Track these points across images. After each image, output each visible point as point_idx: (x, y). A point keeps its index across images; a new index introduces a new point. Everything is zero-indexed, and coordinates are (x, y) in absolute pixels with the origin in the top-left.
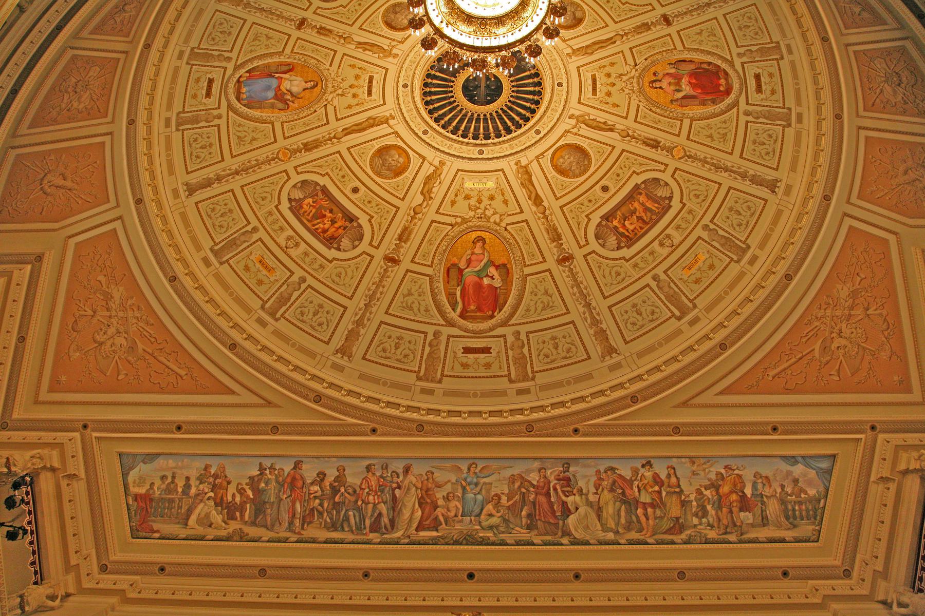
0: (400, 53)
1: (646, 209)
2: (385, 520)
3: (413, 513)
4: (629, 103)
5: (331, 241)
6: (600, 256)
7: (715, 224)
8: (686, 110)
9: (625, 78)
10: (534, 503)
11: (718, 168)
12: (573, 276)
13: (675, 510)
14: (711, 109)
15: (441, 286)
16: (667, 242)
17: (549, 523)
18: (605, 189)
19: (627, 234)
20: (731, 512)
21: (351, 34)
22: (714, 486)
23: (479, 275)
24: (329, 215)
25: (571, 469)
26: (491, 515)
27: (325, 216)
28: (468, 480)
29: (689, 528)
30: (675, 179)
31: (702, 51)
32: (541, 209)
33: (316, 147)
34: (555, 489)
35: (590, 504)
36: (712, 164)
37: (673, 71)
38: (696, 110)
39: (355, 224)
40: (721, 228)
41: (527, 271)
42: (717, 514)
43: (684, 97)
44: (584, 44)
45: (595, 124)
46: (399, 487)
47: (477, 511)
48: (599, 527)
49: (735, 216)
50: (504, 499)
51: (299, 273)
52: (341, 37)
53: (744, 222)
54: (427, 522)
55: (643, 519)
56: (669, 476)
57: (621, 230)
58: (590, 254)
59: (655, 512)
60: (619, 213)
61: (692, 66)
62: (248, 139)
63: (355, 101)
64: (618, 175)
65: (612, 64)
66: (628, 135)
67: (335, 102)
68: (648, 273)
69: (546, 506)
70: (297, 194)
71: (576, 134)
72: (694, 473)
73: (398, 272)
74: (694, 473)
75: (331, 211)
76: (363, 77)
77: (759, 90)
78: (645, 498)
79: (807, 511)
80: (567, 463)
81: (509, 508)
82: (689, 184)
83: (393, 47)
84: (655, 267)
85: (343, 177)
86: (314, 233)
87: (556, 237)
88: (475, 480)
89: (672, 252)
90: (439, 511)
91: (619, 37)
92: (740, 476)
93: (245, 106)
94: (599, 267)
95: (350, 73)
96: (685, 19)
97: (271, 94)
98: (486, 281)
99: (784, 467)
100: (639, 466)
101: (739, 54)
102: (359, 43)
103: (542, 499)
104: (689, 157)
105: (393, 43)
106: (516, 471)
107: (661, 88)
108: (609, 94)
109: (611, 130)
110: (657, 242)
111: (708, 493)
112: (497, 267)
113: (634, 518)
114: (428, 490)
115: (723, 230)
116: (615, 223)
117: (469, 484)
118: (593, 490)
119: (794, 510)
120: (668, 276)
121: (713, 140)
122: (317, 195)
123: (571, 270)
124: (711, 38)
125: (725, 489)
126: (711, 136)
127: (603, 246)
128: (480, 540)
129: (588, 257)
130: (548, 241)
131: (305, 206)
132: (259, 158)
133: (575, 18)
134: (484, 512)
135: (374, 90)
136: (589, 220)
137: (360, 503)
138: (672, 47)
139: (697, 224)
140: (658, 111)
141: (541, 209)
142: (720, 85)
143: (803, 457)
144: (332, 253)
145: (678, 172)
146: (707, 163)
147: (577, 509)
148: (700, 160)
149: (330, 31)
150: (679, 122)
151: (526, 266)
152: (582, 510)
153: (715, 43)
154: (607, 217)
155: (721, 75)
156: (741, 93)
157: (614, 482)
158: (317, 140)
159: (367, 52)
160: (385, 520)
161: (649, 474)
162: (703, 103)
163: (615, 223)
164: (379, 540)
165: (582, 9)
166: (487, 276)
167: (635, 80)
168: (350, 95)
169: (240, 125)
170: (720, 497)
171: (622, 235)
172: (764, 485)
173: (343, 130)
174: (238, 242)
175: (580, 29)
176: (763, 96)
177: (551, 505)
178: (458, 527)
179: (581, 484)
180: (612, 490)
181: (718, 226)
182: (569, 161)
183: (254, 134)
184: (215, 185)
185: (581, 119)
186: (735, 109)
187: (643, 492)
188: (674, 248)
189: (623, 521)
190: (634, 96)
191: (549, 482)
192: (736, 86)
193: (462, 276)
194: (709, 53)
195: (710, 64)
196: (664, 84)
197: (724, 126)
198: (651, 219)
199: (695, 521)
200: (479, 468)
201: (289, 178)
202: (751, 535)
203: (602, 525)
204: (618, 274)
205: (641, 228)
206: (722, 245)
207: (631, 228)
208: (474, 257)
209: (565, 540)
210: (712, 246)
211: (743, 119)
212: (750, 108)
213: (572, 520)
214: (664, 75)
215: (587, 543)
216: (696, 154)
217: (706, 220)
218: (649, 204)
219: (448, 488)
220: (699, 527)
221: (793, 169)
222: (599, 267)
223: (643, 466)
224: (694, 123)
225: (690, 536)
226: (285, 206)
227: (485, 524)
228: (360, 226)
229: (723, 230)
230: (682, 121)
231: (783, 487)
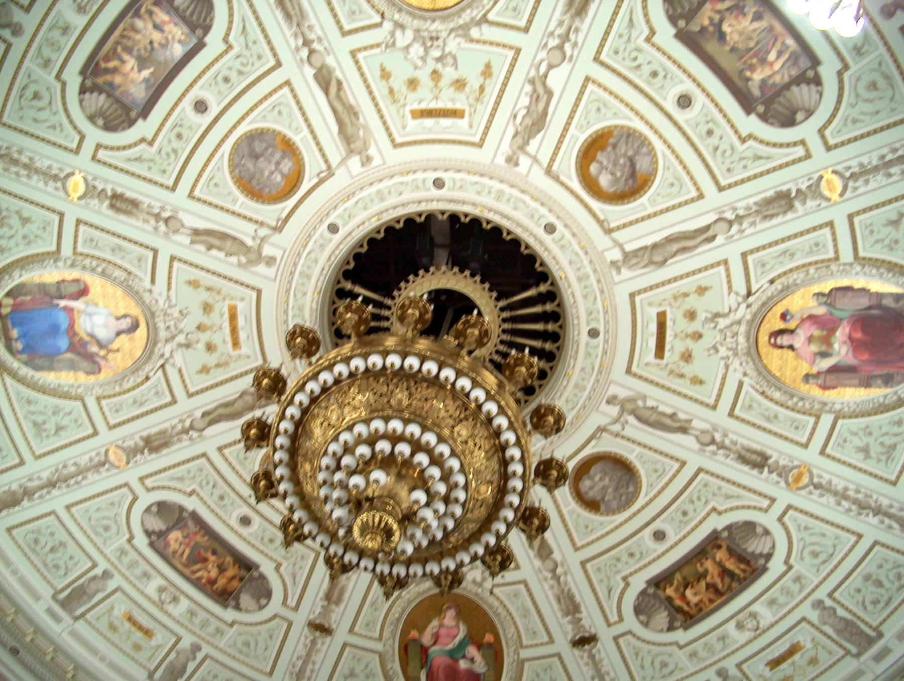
0: (278, 254)
1: (725, 572)
4: (724, 378)
5: (225, 597)
6: (639, 638)
7: (834, 600)
8: (831, 395)
9: (723, 323)
11: (862, 507)
12: (595, 663)
14: (878, 393)
15: (397, 666)
16: (751, 624)
18: (659, 536)
19: (686, 608)
21: (175, 210)
23: (455, 654)
24: (212, 558)
27: (205, 560)
30: (783, 525)
32: (550, 564)
33: (166, 445)
36: (855, 502)
37: (821, 311)
38: (850, 395)
39: (256, 574)
40: (843, 606)
41: (524, 654)
44: (649, 241)
45: (654, 417)
49: (873, 588)
51: (187, 641)
52: (157, 216)
53: (883, 600)
57: (678, 602)
58: (623, 635)
60: (678, 577)
61: (864, 302)
62: (51, 426)
63: (212, 359)
64: (685, 514)
65: (702, 291)
66: (713, 442)
67: (178, 359)
68: (710, 665)
70: (157, 524)
71: (617, 435)
73: (329, 648)
75: (214, 553)
76: (217, 308)
82: (805, 535)
83: (263, 239)
84: (724, 658)
85: (222, 498)
86: (196, 583)
87: (572, 608)
89: (755, 638)
91: (722, 226)
93: (26, 363)
94: (637, 654)
95: (192, 300)
96: (872, 185)
97: (63, 343)
98: (463, 664)
102: (196, 232)
104: (817, 486)
105: (263, 232)
107: (791, 347)
108: (687, 357)
109: (683, 430)
110: (732, 623)
112: (479, 647)
115: (847, 609)
116: (670, 591)
120: (741, 671)
122: (186, 525)
123: (592, 657)
127: (646, 625)
129: (621, 640)
130: (559, 614)
131: (172, 543)
132: (78, 460)
133: (633, 174)
135: (242, 335)
136: (627, 585)
138: (831, 255)
139: (805, 598)
140: (777, 395)
141: (550, 564)
144: (230, 614)
145: (791, 512)
146: (846, 497)
148: (835, 493)
149: (135, 204)
150: (812, 420)
151: (522, 646)
154: (659, 582)
158: (163, 433)
159: (214, 252)
162: (867, 383)
163: (670, 591)
165: (652, 152)
166: (464, 657)
167: (743, 329)
168: (201, 346)
169: (29, 402)
171: (679, 610)
173: (204, 415)
174: (90, 591)
175: (643, 204)
181: (838, 602)
182: (601, 485)
183: (58, 418)
184: (25, 503)
185: (629, 406)
188: (759, 632)
190: (735, 364)
193: (427, 656)
196: (798, 342)
197: (896, 430)
198: (730, 588)
201: (135, 499)
204: (664, 665)
205: (711, 601)
206: (838, 632)
207: (694, 600)
208: (443, 631)
210: (821, 632)
214: (803, 321)
216: (830, 482)
217: (821, 594)
218: (730, 565)
222: (637, 654)
224: (840, 422)
226: (141, 541)
228: (262, 577)
229: (847, 609)
230: (818, 417)
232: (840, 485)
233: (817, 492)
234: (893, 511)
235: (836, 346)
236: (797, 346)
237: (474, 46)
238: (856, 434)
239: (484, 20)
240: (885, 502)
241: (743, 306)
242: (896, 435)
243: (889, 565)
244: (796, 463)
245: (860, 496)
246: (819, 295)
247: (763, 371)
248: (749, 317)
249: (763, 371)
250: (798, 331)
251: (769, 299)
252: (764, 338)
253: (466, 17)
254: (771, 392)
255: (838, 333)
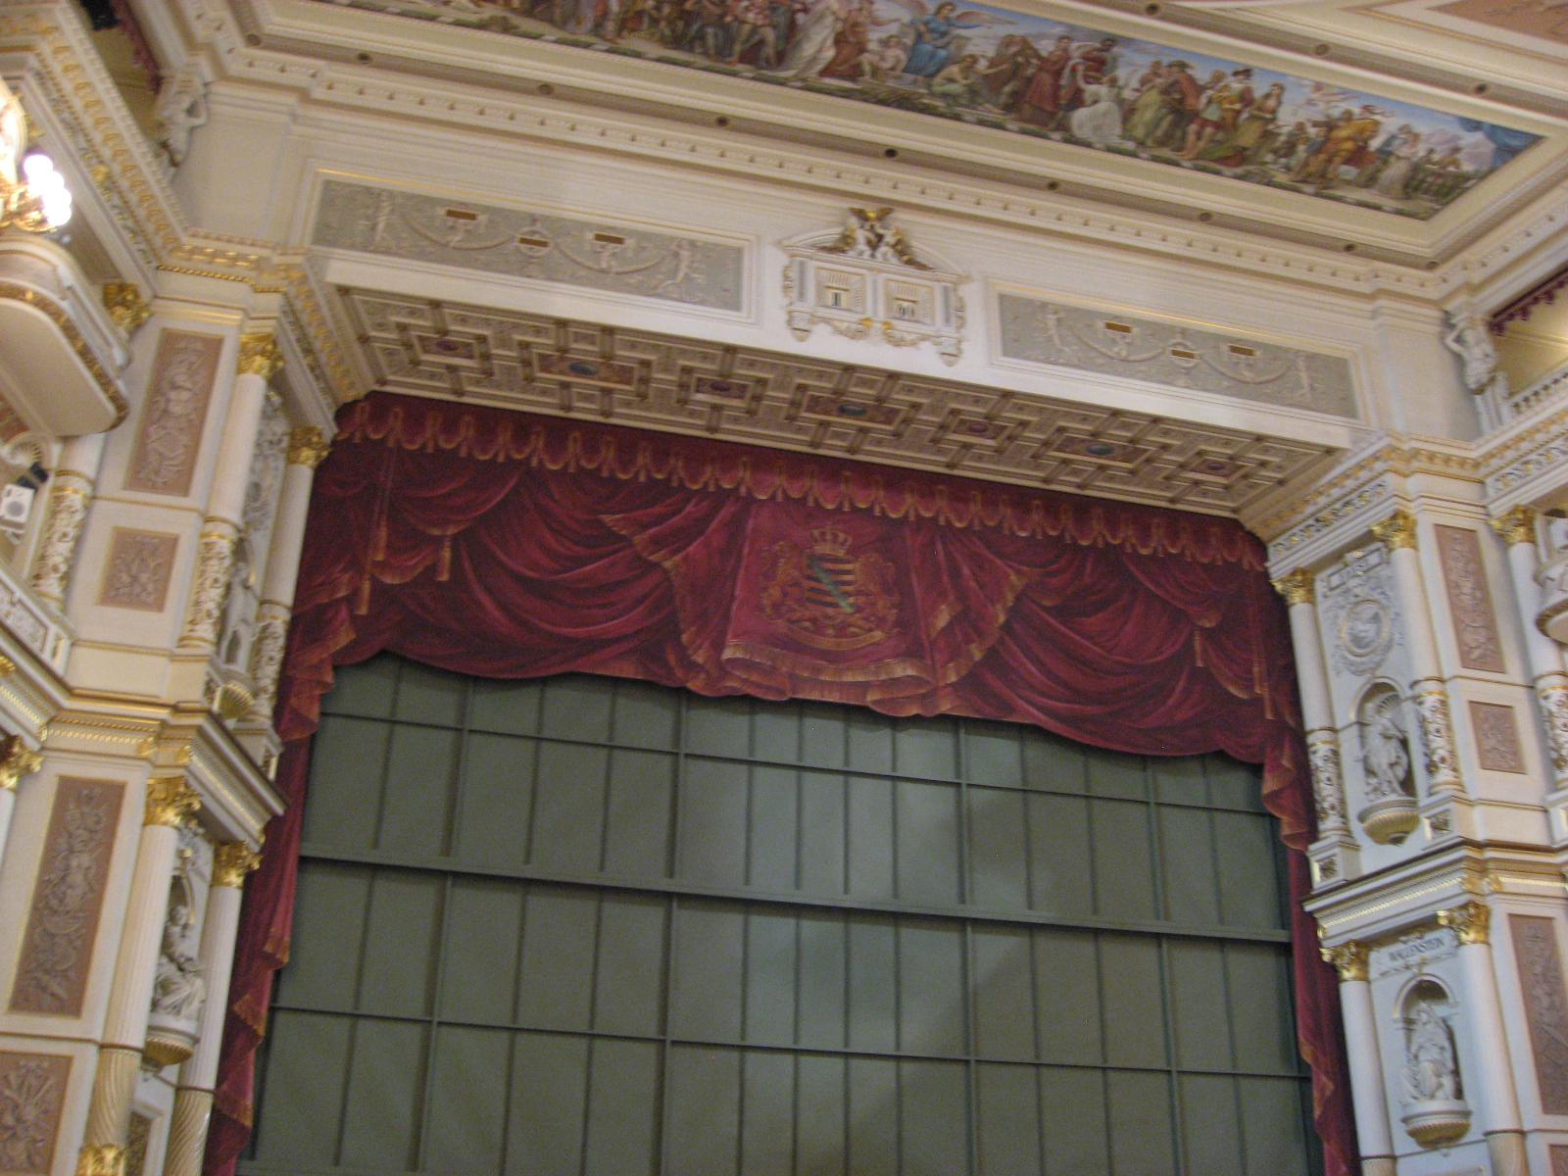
2: (769, 51)
3: (820, 50)
10: (1029, 80)
13: (1248, 137)
17: (1043, 110)
20: (1330, 161)
22: (1330, 126)
25: (1115, 50)
26: (951, 80)
28: (932, 25)
29: (1251, 163)
34: (1074, 70)
35: (1120, 101)
42: (1307, 158)
46: (805, 10)
47: (931, 69)
48: (1118, 131)
50: (982, 66)
54: (840, 68)
55: (1191, 138)
56: (1267, 96)
59: (1214, 134)
69: (1047, 88)
72: (1310, 102)
74: (1310, 102)
78: (1212, 114)
79: (1444, 185)
80: (1110, 41)
81: (986, 77)
88: (943, 28)
90: (866, 59)
92: (1377, 123)
99: (1455, 129)
100: (1229, 71)
103: (1046, 79)
106: (1019, 30)
111: (1312, 131)
113: (1178, 134)
114: (855, 25)
117: (932, 31)
118: (1134, 83)
119: (1423, 181)
125: (1343, 133)
128: (921, 107)
134: (945, 73)
137: (728, 19)
143: (1494, 127)
147: (1095, 102)
152: (1102, 106)
157: (1176, 83)
160: (769, 51)
161: (1237, 86)
164: (750, 75)
170: (1327, 139)
172: (1405, 142)
177: (1057, 88)
178: (891, 83)
179: (1121, 73)
180: (1165, 92)
187: (1213, 107)
189: (1159, 133)
191: (1069, 58)
199: (1269, 157)
200: (958, 12)
202: (1338, 193)
203: (1124, 130)
209: (1057, 136)
213: (1079, 116)
215: (1089, 145)
219: (893, 29)
220: (1272, 166)
223: (1236, 74)
225: (1250, 172)
227: (937, 89)
231: (1431, 151)
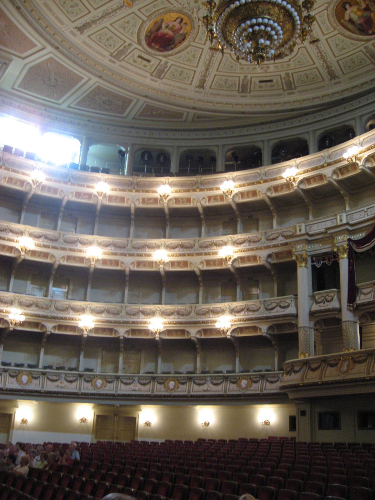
9: (195, 10)
31: (182, 51)
36: (110, 13)
37: (181, 32)
38: (148, 26)
43: (160, 27)
53: (65, 5)
61: (176, 41)
77: (140, 57)
101: (168, 62)
104: (122, 7)
107: (175, 21)
121: (124, 22)
124: (187, 58)
126: (128, 22)
138: (196, 41)
140: (162, 11)
142: (156, 44)
146: (113, 12)
150: (147, 15)
153: (182, 58)
155: (161, 49)
156: (144, 49)
167: (190, 13)
176: (135, 56)
186: (136, 41)
190: (179, 6)
192: (150, 50)
194: (178, 52)
195: (172, 49)
211: (128, 42)
212: (132, 48)
216: (121, 10)
221: (84, 42)
230: (148, 17)
232: (119, 12)
233: (120, 6)
234: (101, 20)
235: (168, 30)
236: (174, 23)
237: (324, 2)
238: (135, 23)
239: (327, 9)
240: (105, 20)
241: (197, 17)
242: (128, 31)
243: (78, 12)
244: (134, 5)
245: (111, 15)
246: (187, 33)
247: (173, 11)
248: (192, 16)
249: (173, 11)
250: (179, 25)
251: (194, 23)
252: (183, 16)
253: (332, 6)
254: (164, 10)
255: (171, 32)
